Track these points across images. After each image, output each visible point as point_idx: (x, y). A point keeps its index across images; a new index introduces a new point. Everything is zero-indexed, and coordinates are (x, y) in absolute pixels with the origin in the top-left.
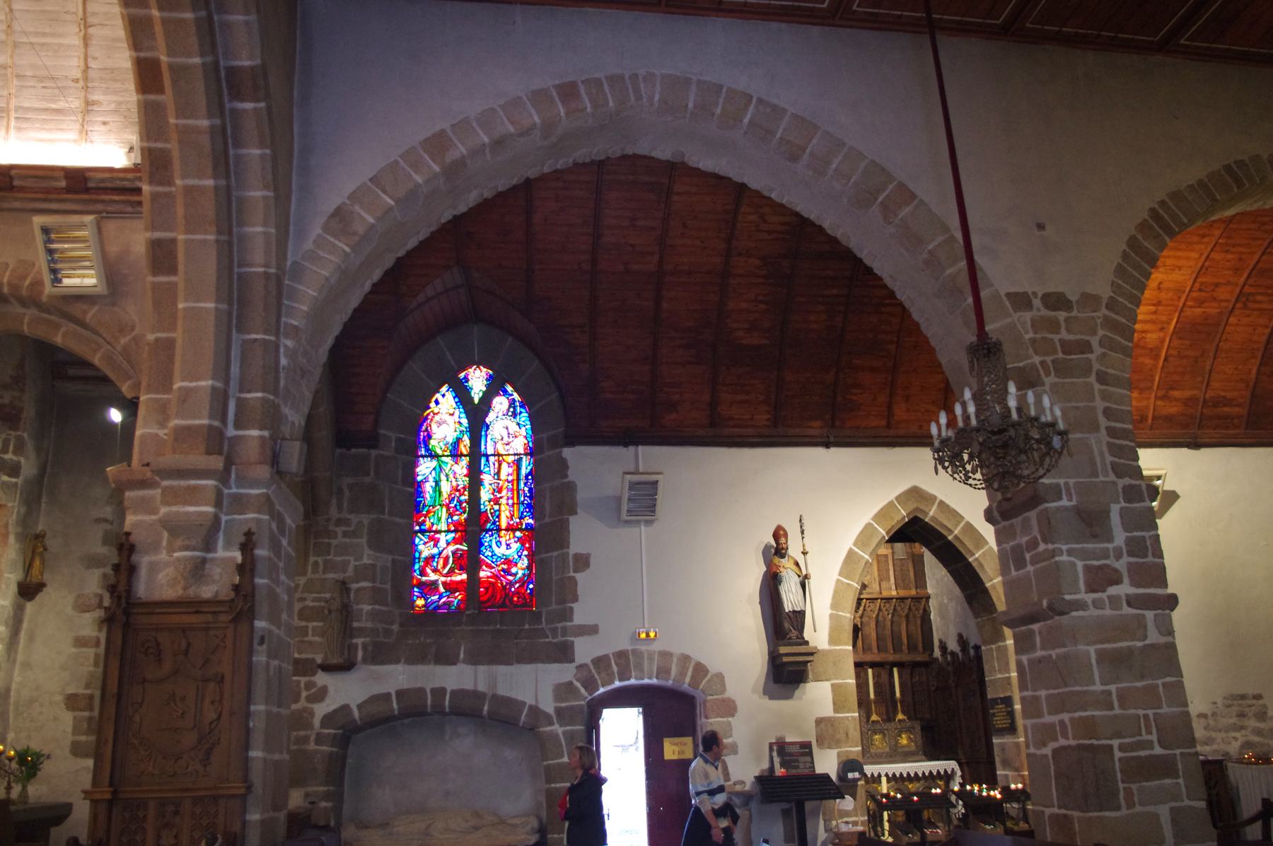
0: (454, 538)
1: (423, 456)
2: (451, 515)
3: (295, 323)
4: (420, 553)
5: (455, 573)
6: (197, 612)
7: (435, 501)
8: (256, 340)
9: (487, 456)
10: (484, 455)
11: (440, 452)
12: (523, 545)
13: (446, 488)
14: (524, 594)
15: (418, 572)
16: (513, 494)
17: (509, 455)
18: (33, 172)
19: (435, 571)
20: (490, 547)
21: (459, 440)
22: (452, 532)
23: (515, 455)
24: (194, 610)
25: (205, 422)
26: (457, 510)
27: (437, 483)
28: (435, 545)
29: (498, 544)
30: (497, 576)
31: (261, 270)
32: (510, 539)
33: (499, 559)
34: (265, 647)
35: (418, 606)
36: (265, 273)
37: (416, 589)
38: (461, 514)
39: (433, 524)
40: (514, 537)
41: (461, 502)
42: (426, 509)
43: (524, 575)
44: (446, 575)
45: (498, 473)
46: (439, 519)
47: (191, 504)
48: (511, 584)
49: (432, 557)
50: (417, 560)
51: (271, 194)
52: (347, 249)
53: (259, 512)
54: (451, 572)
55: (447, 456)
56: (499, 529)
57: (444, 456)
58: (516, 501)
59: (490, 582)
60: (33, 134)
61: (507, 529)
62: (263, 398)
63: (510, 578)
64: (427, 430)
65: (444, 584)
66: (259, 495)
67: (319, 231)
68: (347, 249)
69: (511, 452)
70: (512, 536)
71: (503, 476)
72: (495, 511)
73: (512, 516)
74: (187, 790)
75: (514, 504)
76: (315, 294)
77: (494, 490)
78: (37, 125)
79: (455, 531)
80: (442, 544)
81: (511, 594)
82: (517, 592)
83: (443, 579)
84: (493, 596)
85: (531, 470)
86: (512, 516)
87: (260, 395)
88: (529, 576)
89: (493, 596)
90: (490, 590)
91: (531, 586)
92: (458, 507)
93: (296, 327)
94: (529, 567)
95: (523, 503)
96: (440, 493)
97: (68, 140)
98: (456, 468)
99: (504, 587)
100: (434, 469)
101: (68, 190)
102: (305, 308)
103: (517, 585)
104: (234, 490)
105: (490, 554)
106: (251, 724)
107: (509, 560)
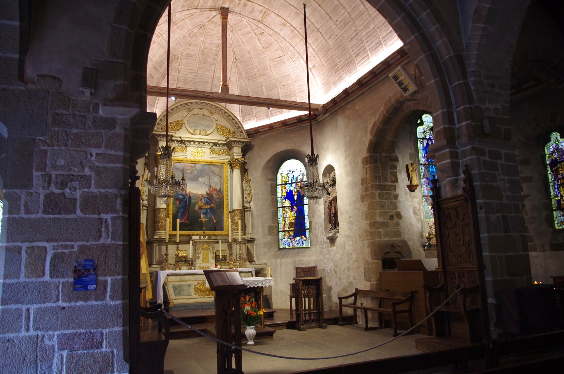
3: (473, 69)
6: (457, 200)
8: (456, 85)
18: (393, 56)
24: (455, 200)
25: (442, 127)
31: (448, 56)
34: (483, 210)
36: (449, 57)
47: (444, 161)
51: (438, 25)
52: (483, 26)
53: (471, 156)
60: (388, 44)
62: (464, 108)
66: (469, 148)
67: (471, 24)
68: (483, 26)
74: (464, 268)
76: (476, 53)
78: (388, 40)
87: (462, 107)
93: (473, 71)
97: (396, 40)
101: (402, 57)
102: (474, 61)
104: (462, 149)
106: (482, 242)
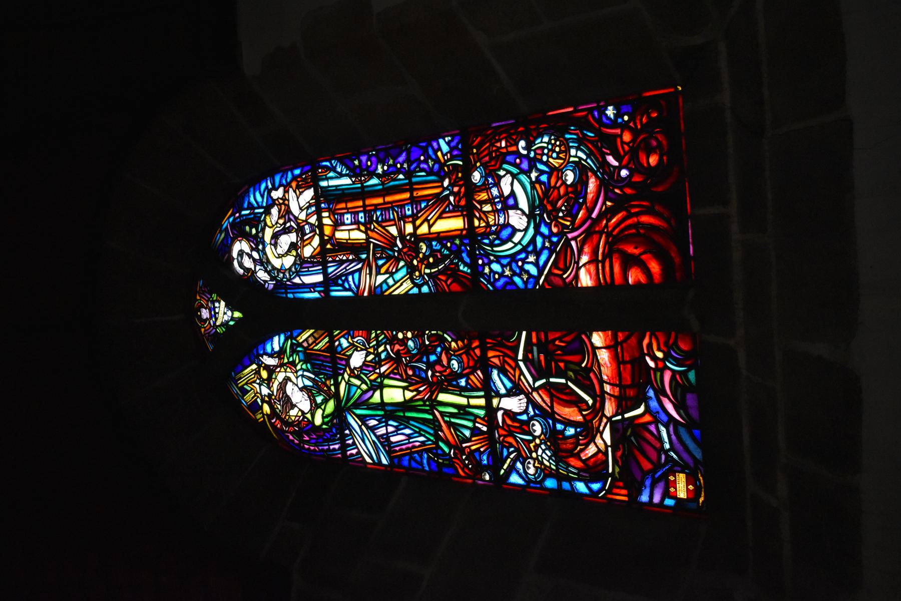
0: (502, 371)
1: (344, 447)
2: (448, 383)
4: (547, 473)
5: (588, 369)
7: (424, 421)
9: (329, 282)
10: (327, 291)
11: (330, 406)
12: (501, 158)
13: (394, 394)
14: (635, 133)
15: (596, 486)
16: (392, 205)
17: (321, 226)
19: (589, 432)
20: (513, 258)
21: (309, 357)
22: (488, 378)
23: (319, 212)
26: (439, 361)
27: (390, 412)
28: (525, 428)
29: (505, 233)
30: (589, 233)
32: (491, 201)
33: (544, 230)
35: (693, 496)
37: (645, 498)
38: (447, 350)
39: (475, 431)
40: (485, 187)
41: (424, 351)
42: (446, 450)
43: (581, 142)
44: (600, 398)
45: (354, 248)
46: (463, 411)
48: (608, 180)
49: (553, 438)
50: (566, 485)
54: (586, 378)
55: (337, 385)
56: (470, 234)
57: (336, 395)
58: (407, 195)
59: (608, 255)
61: (468, 211)
63: (592, 185)
64: (299, 434)
65: (623, 405)
69: (313, 220)
70: (483, 196)
71: (358, 236)
72: (433, 253)
73: (439, 200)
75: (414, 201)
77: (388, 258)
79: (485, 366)
80: (514, 404)
81: (637, 179)
82: (631, 158)
83: (609, 409)
84: (643, 237)
85: (342, 163)
86: (439, 200)
88: (582, 124)
89: (643, 237)
90: (631, 250)
91: (610, 112)
92: (433, 358)
94: (558, 129)
95: (409, 174)
96: (406, 405)
98: (357, 360)
99: (620, 204)
100: (363, 419)
103: (611, 159)
105: (532, 258)
107: (546, 193)
